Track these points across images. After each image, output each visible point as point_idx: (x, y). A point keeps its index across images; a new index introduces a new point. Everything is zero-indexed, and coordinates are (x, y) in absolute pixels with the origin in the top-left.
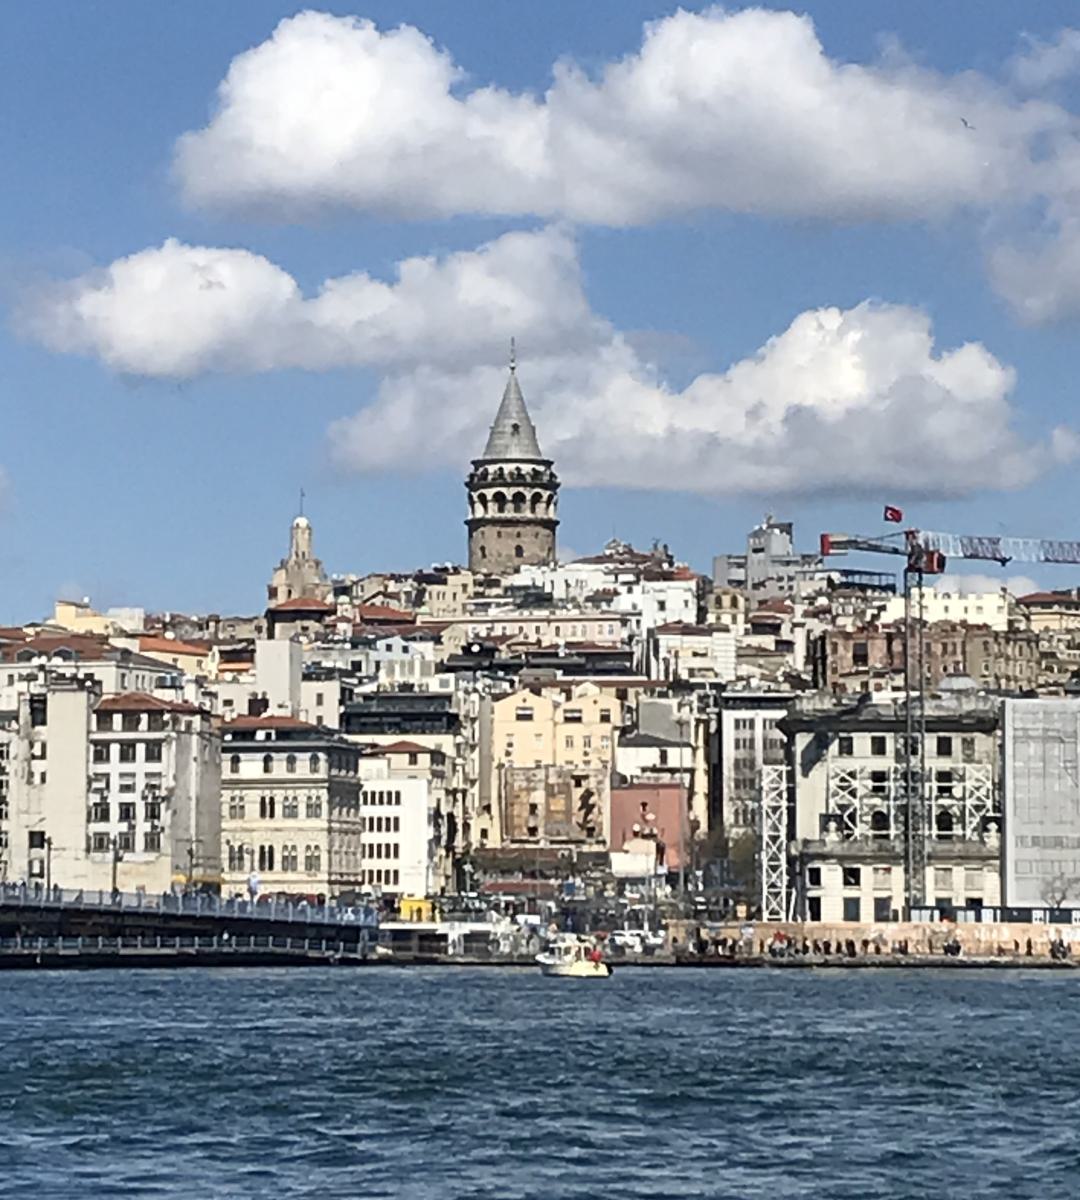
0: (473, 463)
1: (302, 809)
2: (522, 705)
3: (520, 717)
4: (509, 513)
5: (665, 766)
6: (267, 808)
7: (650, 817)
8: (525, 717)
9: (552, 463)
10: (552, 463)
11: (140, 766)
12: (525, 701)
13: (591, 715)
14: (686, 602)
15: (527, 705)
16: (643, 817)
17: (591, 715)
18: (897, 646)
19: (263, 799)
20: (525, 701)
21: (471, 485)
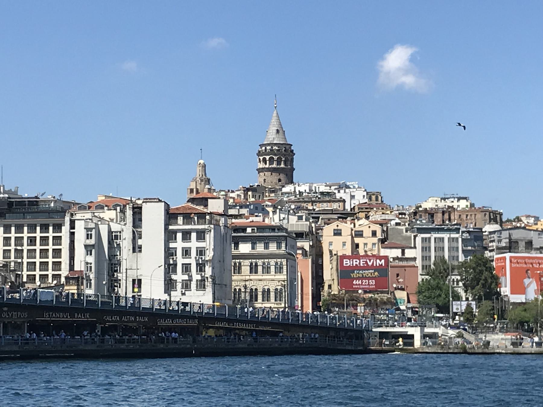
0: (260, 145)
1: (273, 269)
2: (336, 228)
3: (335, 234)
4: (274, 165)
5: (404, 257)
6: (253, 269)
7: (401, 280)
8: (337, 233)
9: (292, 145)
10: (292, 145)
11: (194, 244)
12: (338, 226)
13: (367, 233)
14: (364, 196)
15: (339, 228)
16: (397, 280)
17: (367, 233)
18: (446, 216)
19: (251, 264)
20: (338, 226)
21: (259, 154)
